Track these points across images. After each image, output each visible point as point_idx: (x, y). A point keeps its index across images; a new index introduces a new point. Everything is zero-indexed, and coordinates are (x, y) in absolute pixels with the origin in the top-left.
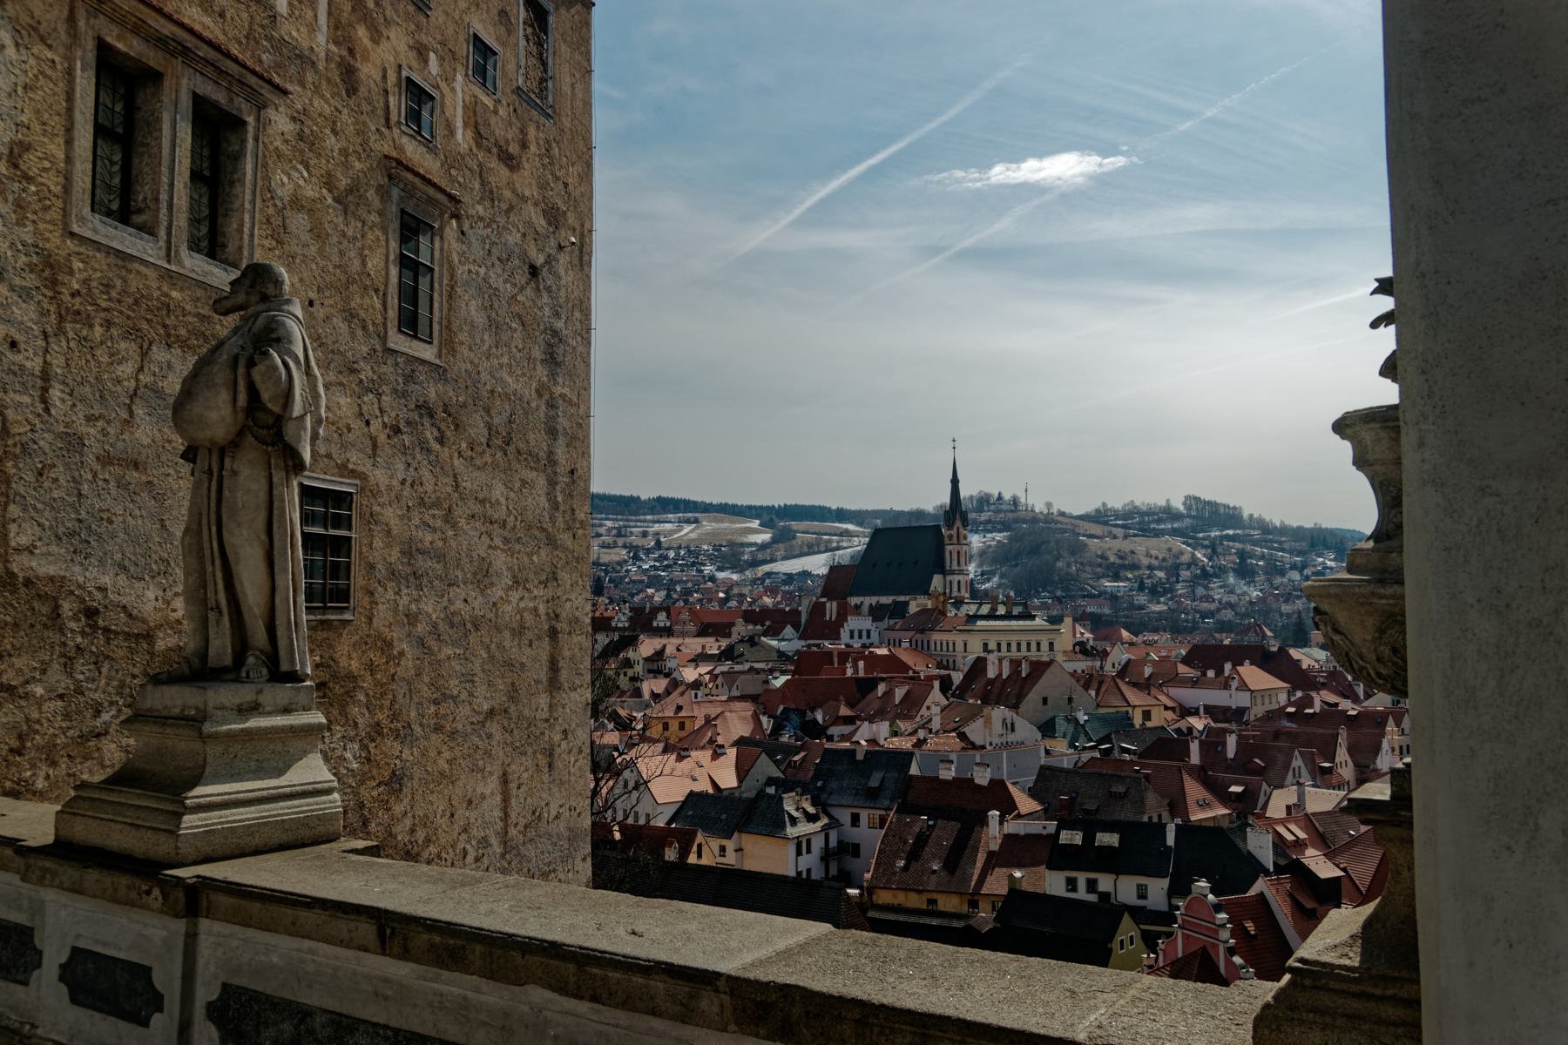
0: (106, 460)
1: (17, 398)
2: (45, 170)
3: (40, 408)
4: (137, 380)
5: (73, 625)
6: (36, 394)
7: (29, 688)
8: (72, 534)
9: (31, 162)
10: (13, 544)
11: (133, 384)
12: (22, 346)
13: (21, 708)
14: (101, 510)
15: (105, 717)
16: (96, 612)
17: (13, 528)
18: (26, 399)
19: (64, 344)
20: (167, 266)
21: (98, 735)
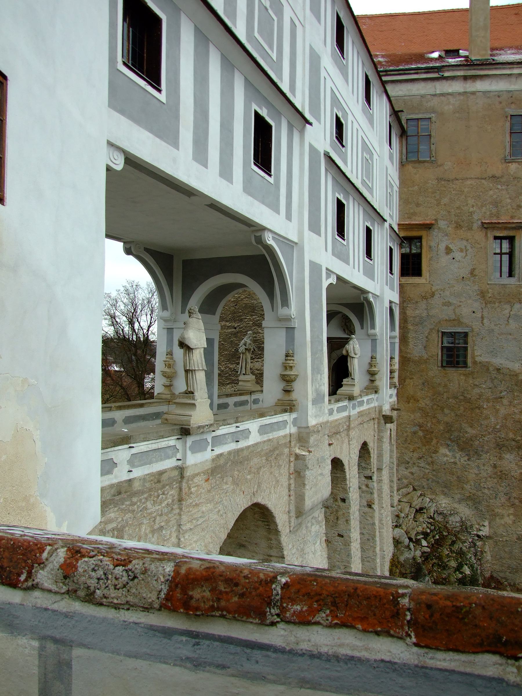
0: (501, 334)
1: (475, 323)
2: (480, 272)
3: (481, 325)
4: (510, 314)
5: (493, 372)
6: (480, 322)
7: (481, 385)
8: (492, 352)
9: (476, 272)
10: (476, 355)
11: (509, 314)
12: (476, 312)
13: (479, 390)
14: (500, 346)
15: (503, 394)
16: (500, 369)
17: (476, 352)
18: (477, 323)
19: (487, 309)
20: (519, 283)
21: (501, 398)
